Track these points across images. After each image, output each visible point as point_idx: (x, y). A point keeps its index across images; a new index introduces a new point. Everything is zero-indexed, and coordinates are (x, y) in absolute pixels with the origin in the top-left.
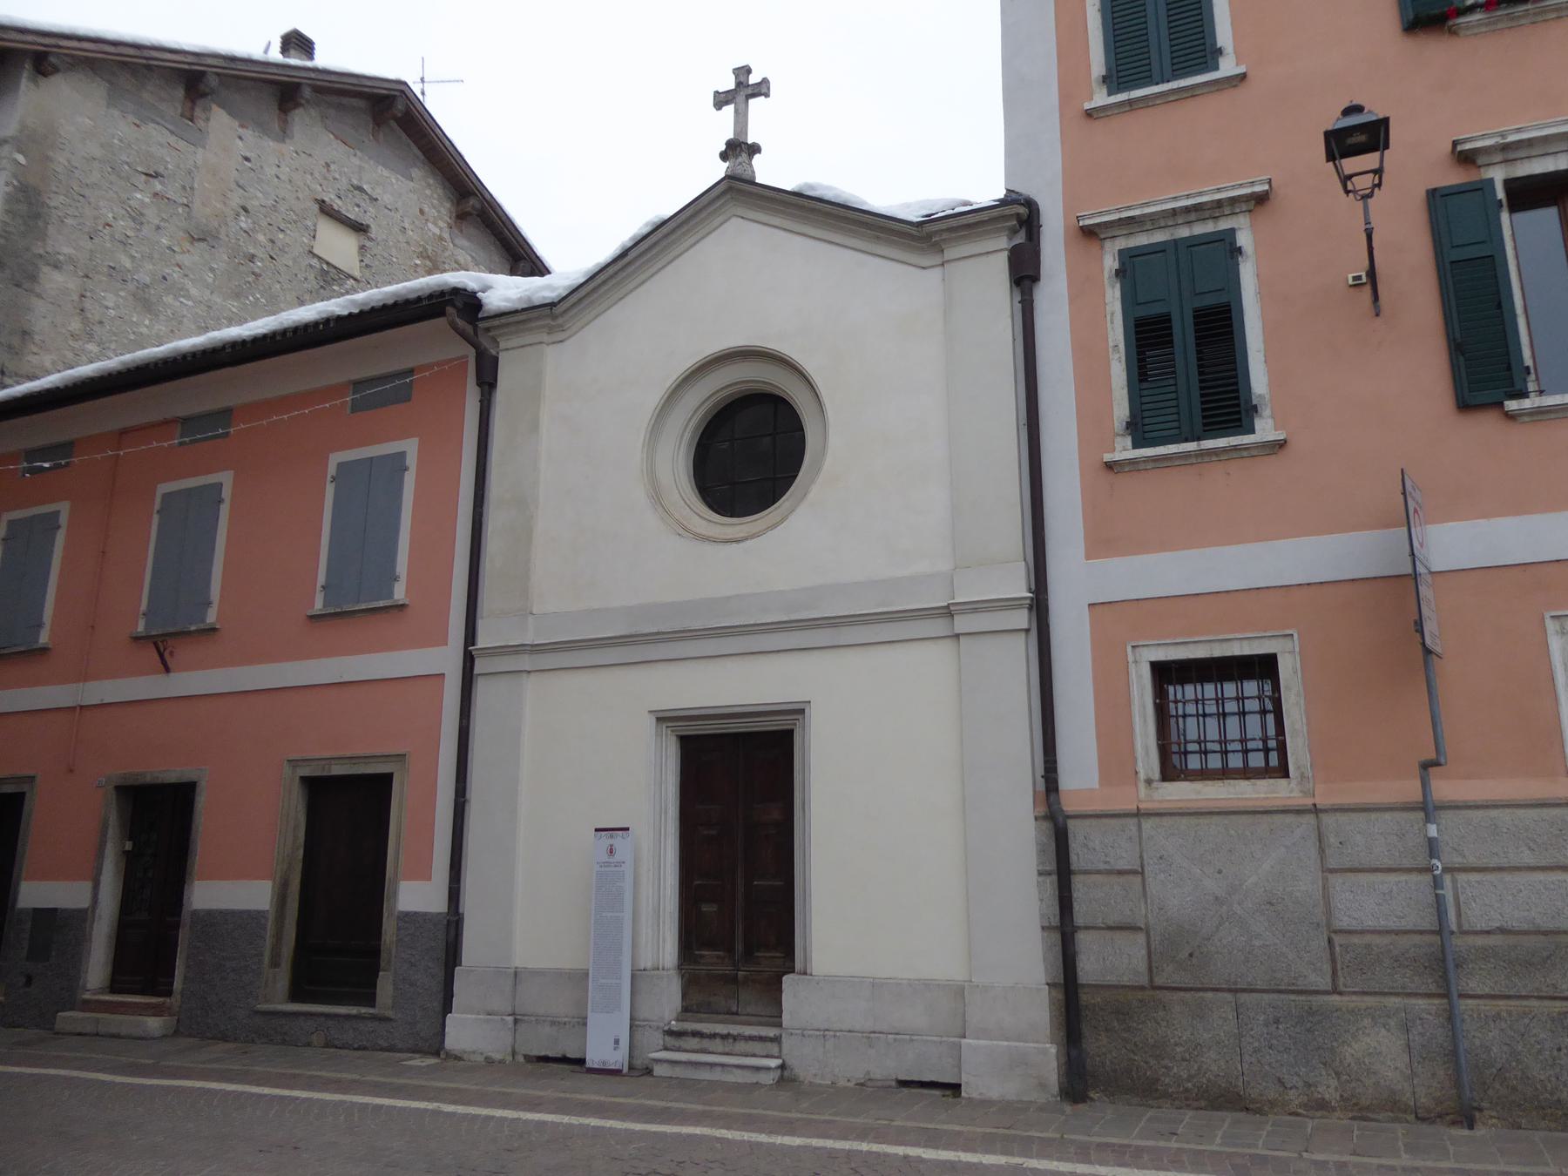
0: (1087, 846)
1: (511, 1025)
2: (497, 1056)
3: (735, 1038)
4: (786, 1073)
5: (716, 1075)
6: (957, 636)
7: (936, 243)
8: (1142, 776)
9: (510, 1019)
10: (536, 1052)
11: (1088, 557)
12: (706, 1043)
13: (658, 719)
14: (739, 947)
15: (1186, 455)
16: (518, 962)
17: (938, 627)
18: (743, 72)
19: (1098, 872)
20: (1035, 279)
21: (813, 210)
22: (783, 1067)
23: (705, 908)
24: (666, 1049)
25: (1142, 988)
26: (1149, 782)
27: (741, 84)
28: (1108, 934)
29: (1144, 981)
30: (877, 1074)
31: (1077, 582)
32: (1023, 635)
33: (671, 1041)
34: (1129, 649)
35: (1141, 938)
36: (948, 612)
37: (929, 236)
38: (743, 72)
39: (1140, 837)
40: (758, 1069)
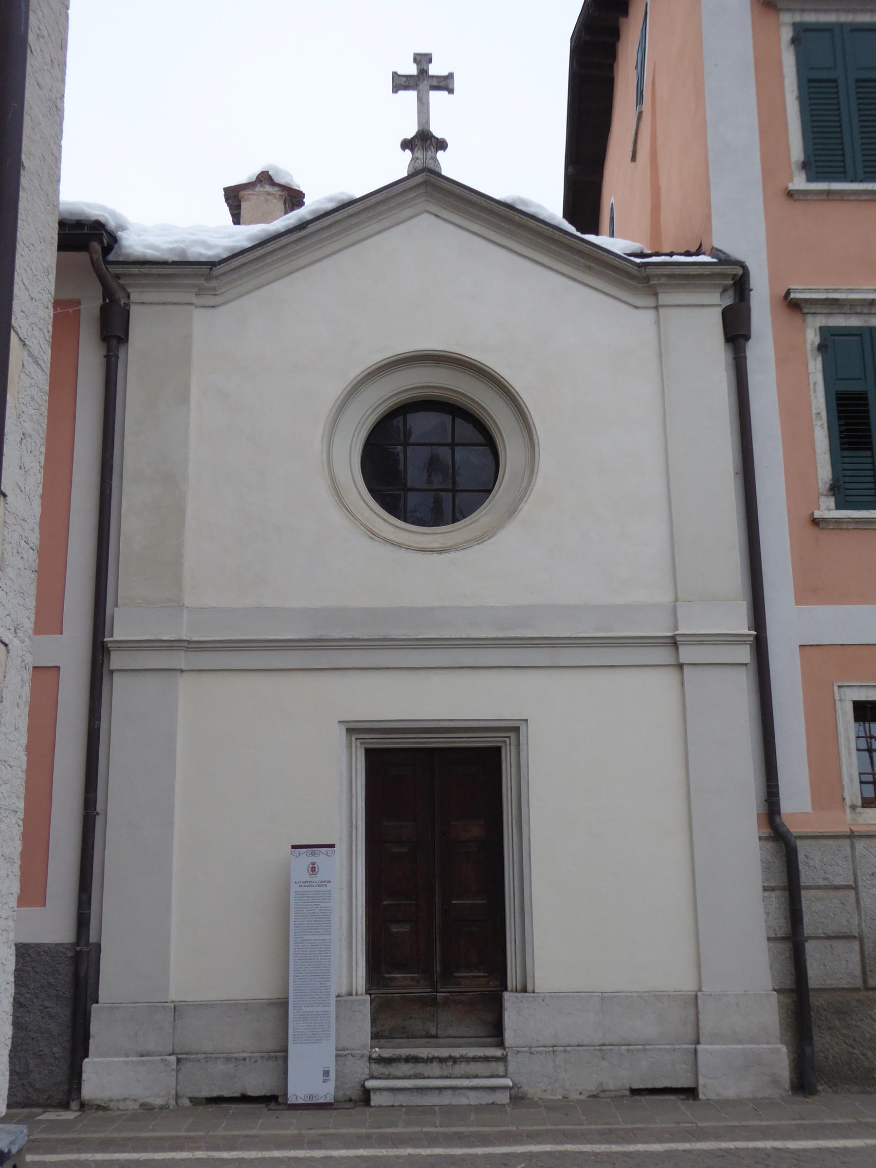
0: (814, 863)
1: (174, 1067)
2: (159, 1102)
3: (454, 1060)
5: (446, 1099)
6: (681, 666)
7: (652, 286)
8: (848, 802)
9: (173, 1058)
10: (206, 1093)
11: (798, 602)
12: (420, 1068)
13: (348, 730)
16: (174, 995)
17: (664, 655)
18: (423, 60)
19: (819, 887)
20: (747, 337)
21: (520, 225)
23: (395, 929)
25: (857, 989)
26: (853, 807)
27: (423, 72)
28: (827, 943)
30: (611, 1084)
31: (792, 624)
33: (377, 1069)
34: (836, 688)
35: (856, 945)
36: (674, 642)
37: (648, 279)
38: (423, 60)
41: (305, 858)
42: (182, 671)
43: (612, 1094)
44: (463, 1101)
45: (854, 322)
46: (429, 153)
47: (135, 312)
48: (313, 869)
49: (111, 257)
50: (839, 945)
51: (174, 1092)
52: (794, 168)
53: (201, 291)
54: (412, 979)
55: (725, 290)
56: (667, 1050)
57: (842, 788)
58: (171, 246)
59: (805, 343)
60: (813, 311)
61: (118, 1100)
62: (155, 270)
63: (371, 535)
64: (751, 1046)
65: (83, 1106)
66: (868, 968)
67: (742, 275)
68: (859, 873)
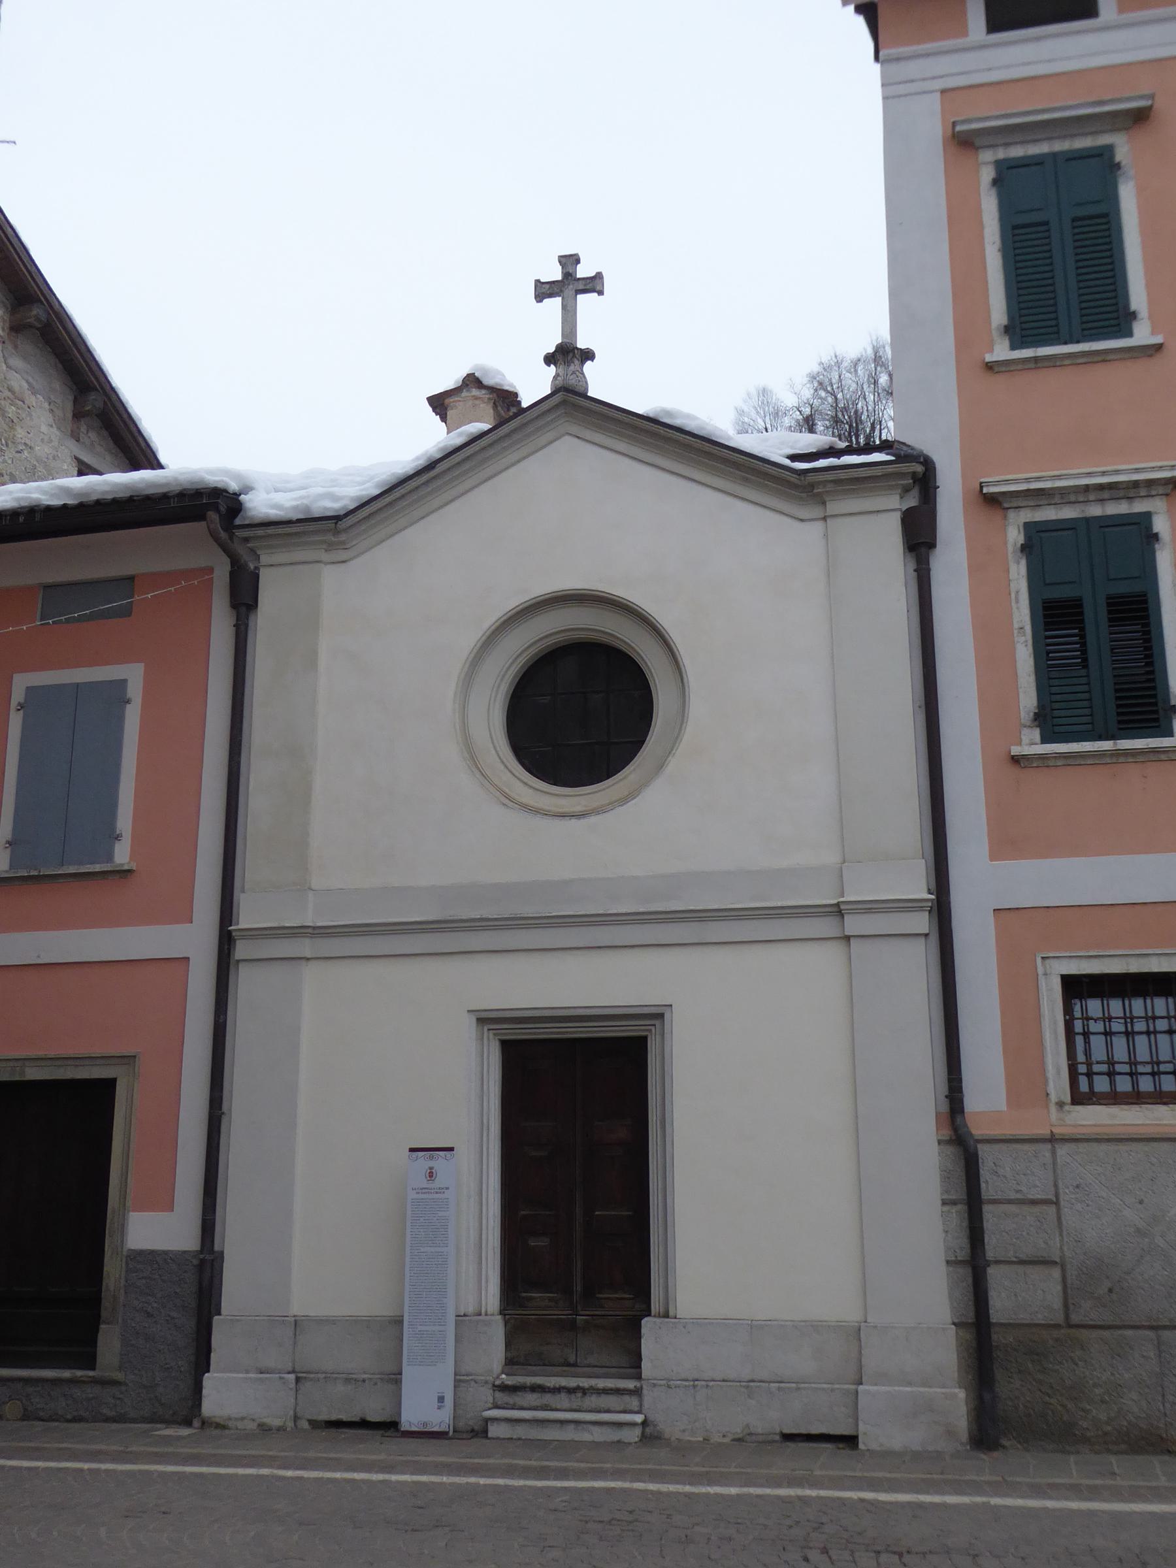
0: (1000, 1173)
1: (293, 1385)
2: (276, 1422)
3: (584, 1391)
4: (648, 1430)
5: (569, 1434)
6: (848, 938)
7: (819, 494)
8: (1053, 1098)
9: (292, 1376)
10: (324, 1417)
12: (548, 1399)
13: (481, 1021)
14: (578, 1287)
15: (1102, 754)
16: (299, 1306)
17: (826, 926)
18: (569, 262)
19: (1010, 1202)
20: (932, 545)
21: (668, 440)
22: (645, 1423)
24: (496, 1407)
25: (1057, 1326)
26: (1060, 1105)
27: (568, 276)
28: (1020, 1269)
29: (1060, 1318)
30: (759, 1427)
31: (985, 884)
32: (923, 940)
33: (502, 1397)
34: (1039, 960)
35: (1056, 1273)
36: (838, 911)
37: (812, 486)
38: (569, 262)
39: (1054, 1163)
40: (620, 1425)
41: (423, 1162)
42: (308, 959)
43: (761, 1438)
44: (586, 1437)
45: (1068, 513)
46: (572, 368)
47: (265, 576)
48: (431, 1175)
49: (238, 521)
50: (1035, 1272)
51: (292, 1413)
52: (995, 333)
53: (330, 547)
54: (550, 1299)
55: (906, 490)
56: (823, 1389)
57: (1046, 1081)
58: (294, 503)
59: (1006, 543)
60: (1015, 505)
61: (236, 1419)
63: (506, 801)
64: (922, 1389)
65: (205, 1423)
66: (1070, 1301)
67: (924, 474)
68: (1060, 1185)
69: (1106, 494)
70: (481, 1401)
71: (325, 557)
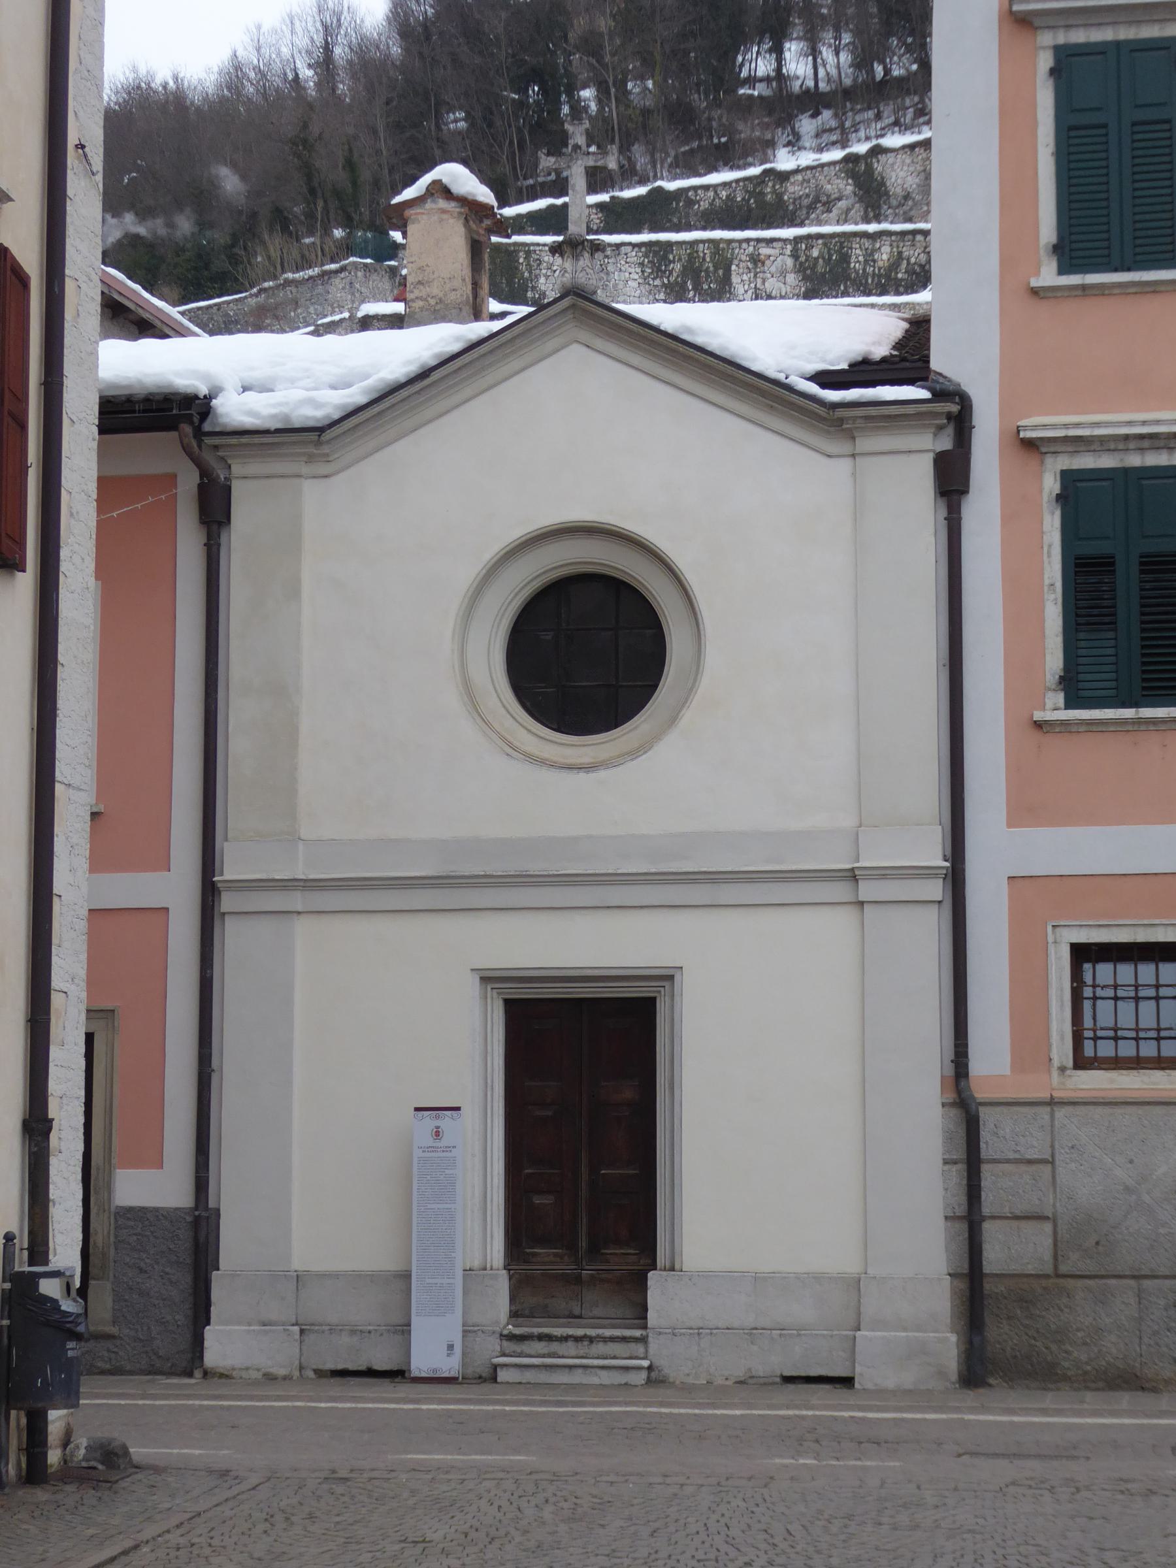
1: (297, 1337)
2: (282, 1372)
3: (591, 1340)
4: (653, 1374)
6: (862, 903)
7: (850, 430)
8: (1056, 1063)
9: (296, 1328)
10: (330, 1366)
11: (1009, 825)
12: (555, 1347)
13: (482, 979)
14: (583, 1243)
15: (1124, 722)
16: (298, 1263)
17: (840, 891)
19: (1008, 1161)
20: (965, 491)
22: (650, 1368)
23: (537, 1200)
24: (504, 1355)
25: (1047, 1276)
26: (1062, 1069)
28: (1014, 1223)
29: (1049, 1269)
30: (760, 1370)
32: (936, 906)
33: (509, 1346)
34: (1050, 929)
35: (1048, 1227)
36: (852, 876)
37: (841, 420)
39: (1052, 1126)
40: (626, 1369)
41: (428, 1122)
42: (299, 913)
43: (762, 1381)
44: (595, 1380)
45: (1107, 462)
46: (581, 263)
47: (237, 489)
48: (437, 1134)
49: (207, 427)
50: (1028, 1227)
51: (297, 1363)
52: (1042, 252)
53: (311, 459)
54: (555, 1255)
55: (940, 428)
56: (824, 1336)
57: (1049, 1046)
58: (274, 411)
59: (1041, 491)
60: (1052, 450)
61: (241, 1369)
62: (257, 440)
63: (510, 751)
64: (917, 1334)
65: (206, 1374)
66: (1060, 1253)
67: (960, 412)
68: (1057, 1146)
69: (1146, 443)
70: (489, 1349)
71: (305, 469)
